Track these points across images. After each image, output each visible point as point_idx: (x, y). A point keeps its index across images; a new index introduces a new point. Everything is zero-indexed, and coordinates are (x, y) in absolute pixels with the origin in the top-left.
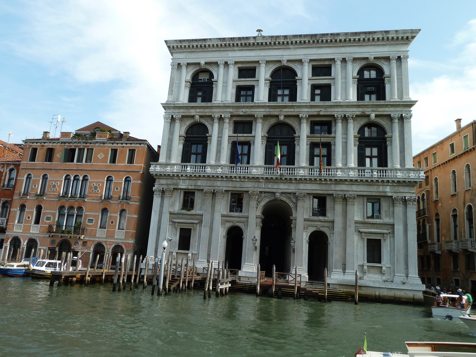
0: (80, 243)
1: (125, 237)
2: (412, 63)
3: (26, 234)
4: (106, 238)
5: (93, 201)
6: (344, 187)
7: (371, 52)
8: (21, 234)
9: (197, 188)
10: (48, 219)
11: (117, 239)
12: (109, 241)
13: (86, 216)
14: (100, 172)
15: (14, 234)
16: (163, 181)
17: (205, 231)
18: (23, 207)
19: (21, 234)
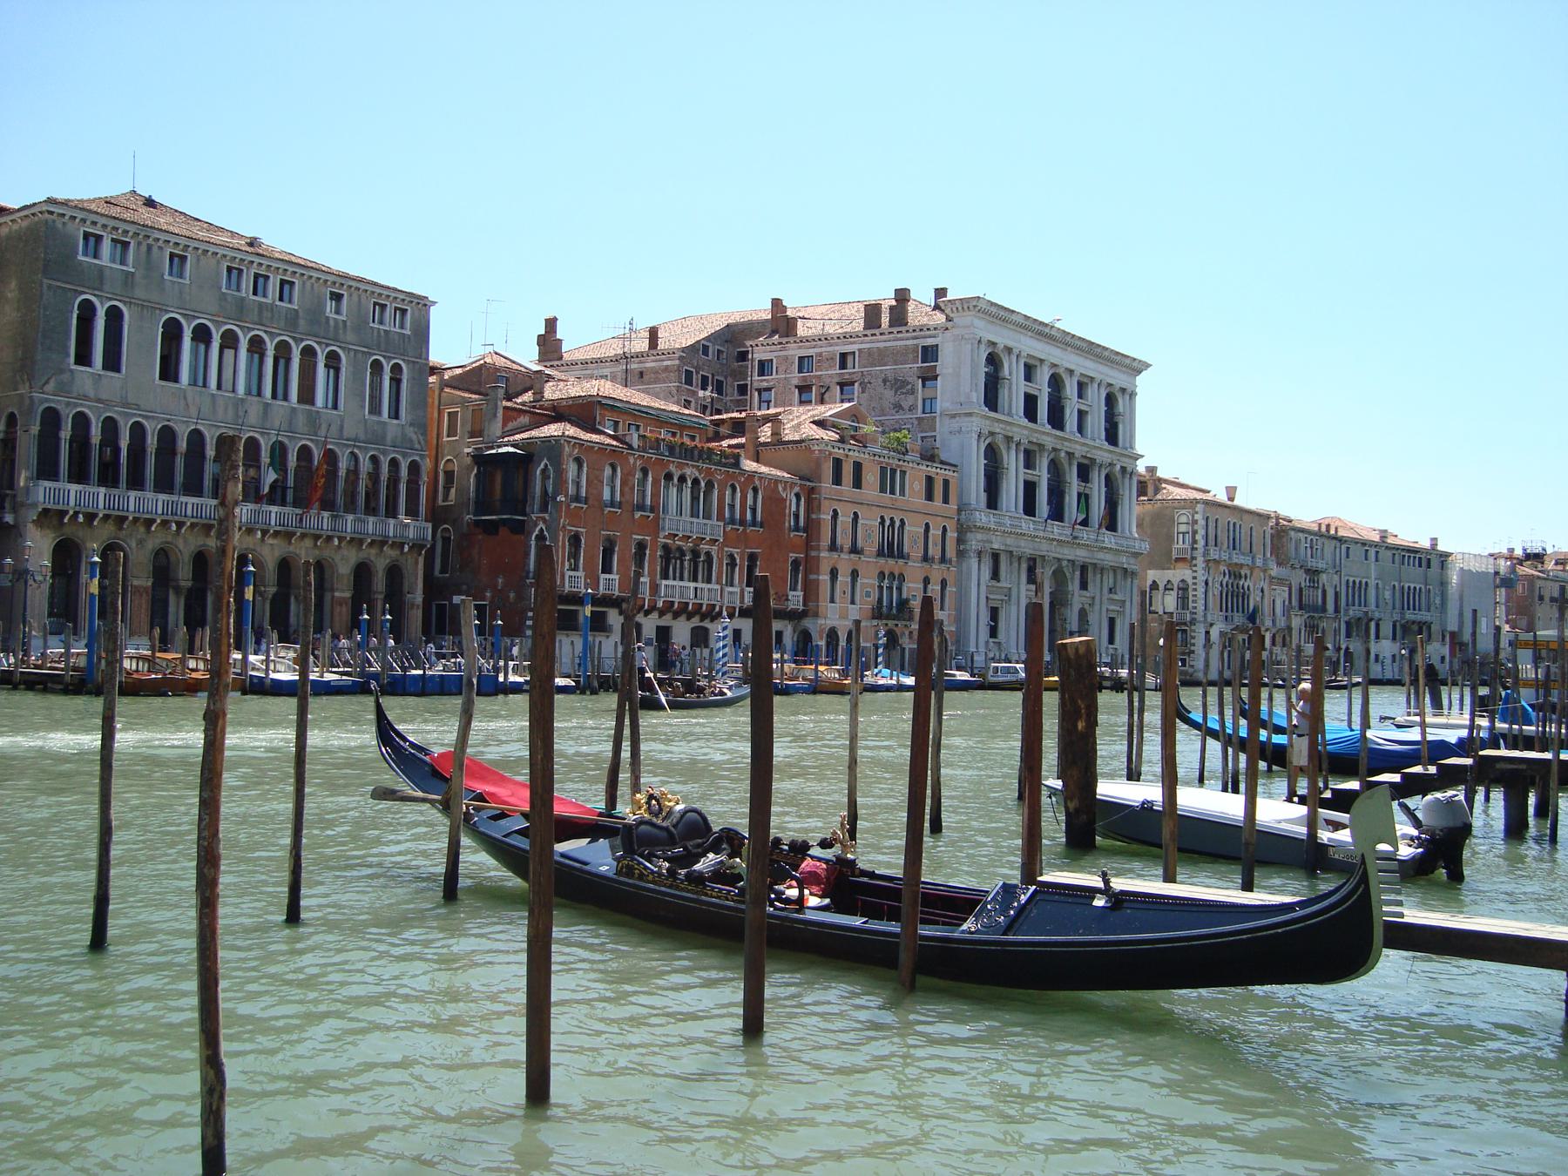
2: (1140, 401)
6: (1101, 555)
7: (1118, 379)
16: (979, 536)
17: (1014, 609)
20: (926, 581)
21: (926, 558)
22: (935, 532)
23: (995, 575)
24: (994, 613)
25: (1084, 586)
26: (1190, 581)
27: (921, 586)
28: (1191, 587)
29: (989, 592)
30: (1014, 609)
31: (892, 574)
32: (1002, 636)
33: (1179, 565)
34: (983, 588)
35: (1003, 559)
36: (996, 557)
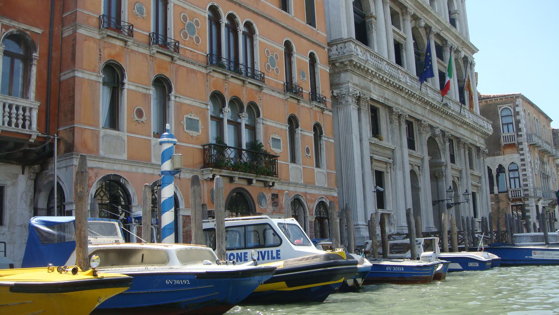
0: (268, 196)
1: (328, 185)
3: (140, 170)
4: (305, 185)
5: (273, 94)
8: (126, 168)
9: (387, 103)
10: (192, 125)
11: (320, 188)
12: (310, 194)
13: (266, 127)
14: (272, 24)
15: (104, 165)
16: (356, 79)
18: (114, 75)
19: (126, 168)
20: (293, 122)
21: (290, 88)
22: (300, 59)
23: (376, 132)
24: (379, 177)
25: (453, 161)
26: (519, 163)
27: (285, 127)
28: (521, 168)
29: (372, 152)
30: (399, 174)
31: (236, 102)
32: (389, 207)
33: (509, 150)
34: (366, 144)
35: (383, 114)
36: (374, 112)
